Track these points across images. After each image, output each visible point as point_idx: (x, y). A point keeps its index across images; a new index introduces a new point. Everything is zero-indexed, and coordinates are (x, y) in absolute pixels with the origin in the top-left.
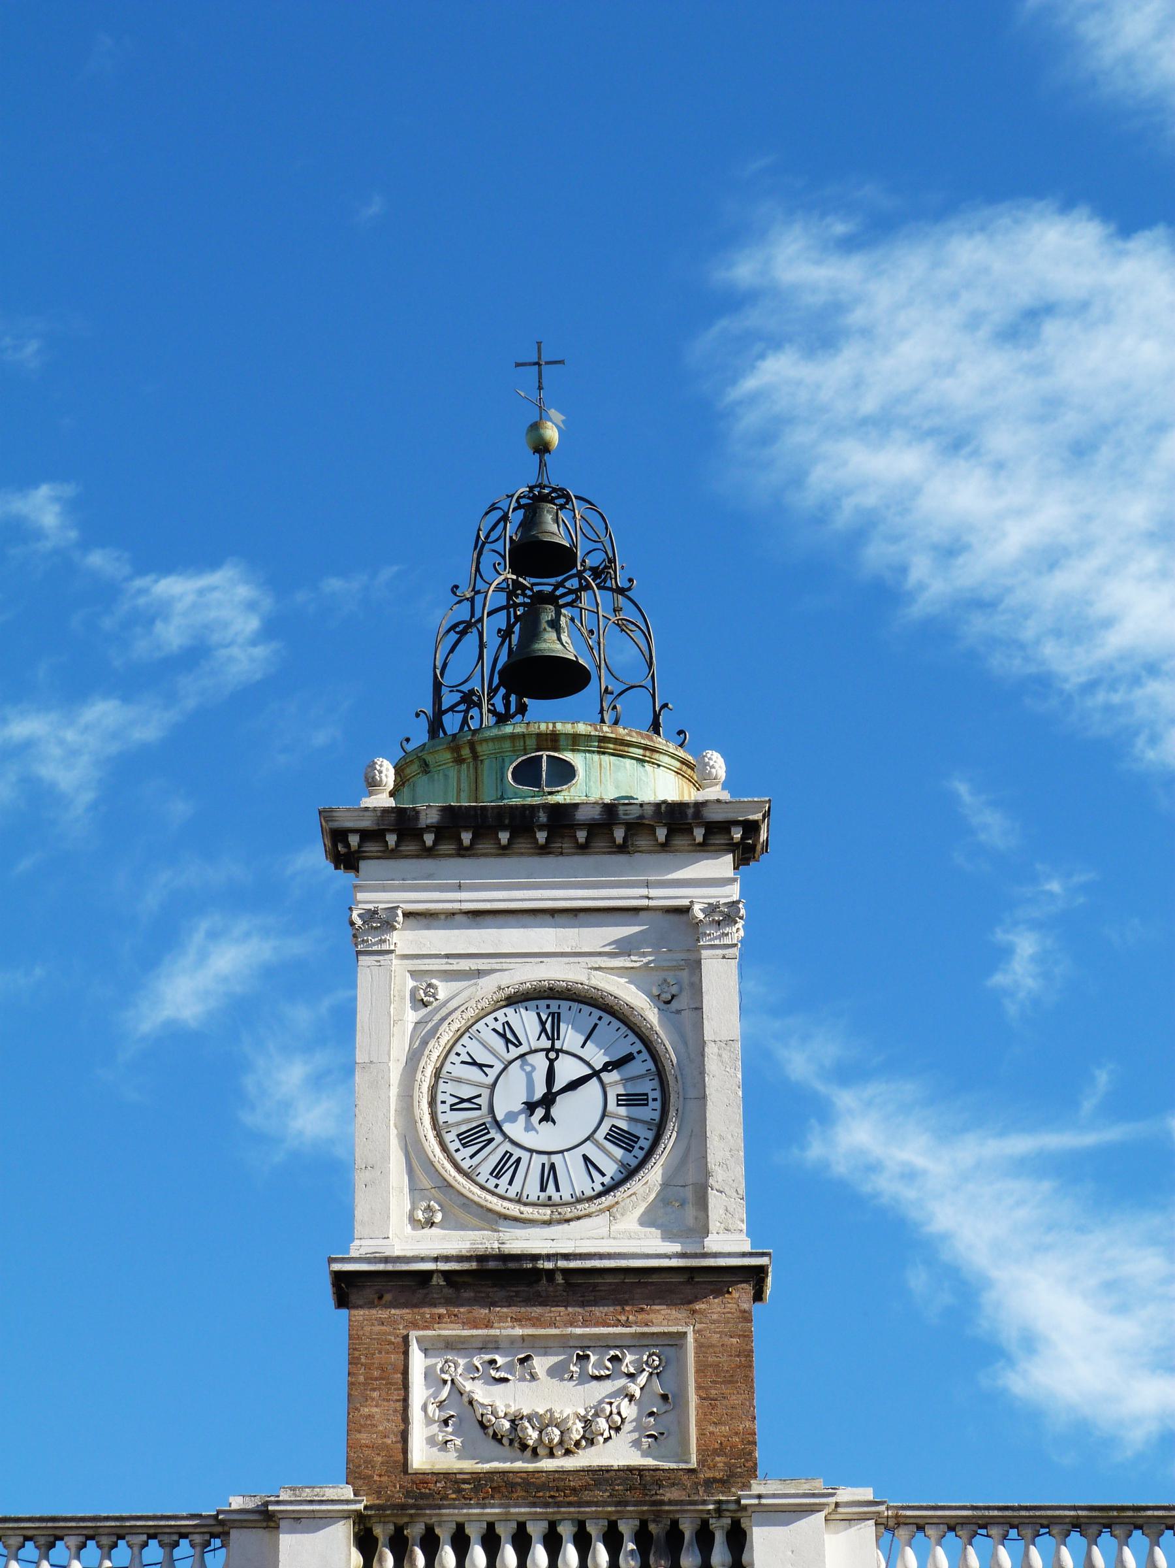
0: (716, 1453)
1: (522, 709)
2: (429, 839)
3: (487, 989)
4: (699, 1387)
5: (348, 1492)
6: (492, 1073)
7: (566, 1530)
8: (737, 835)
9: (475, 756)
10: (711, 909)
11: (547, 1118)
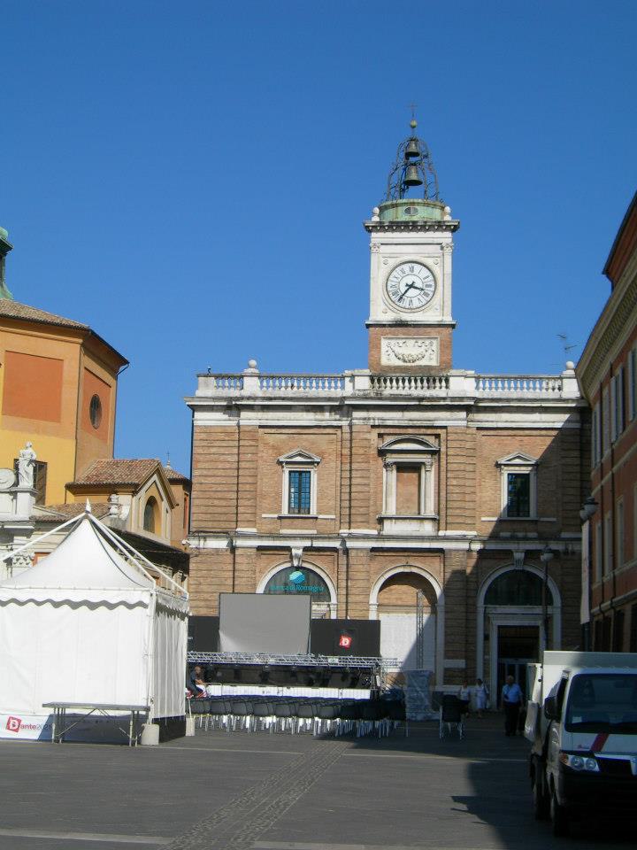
3: (399, 261)
5: (368, 371)
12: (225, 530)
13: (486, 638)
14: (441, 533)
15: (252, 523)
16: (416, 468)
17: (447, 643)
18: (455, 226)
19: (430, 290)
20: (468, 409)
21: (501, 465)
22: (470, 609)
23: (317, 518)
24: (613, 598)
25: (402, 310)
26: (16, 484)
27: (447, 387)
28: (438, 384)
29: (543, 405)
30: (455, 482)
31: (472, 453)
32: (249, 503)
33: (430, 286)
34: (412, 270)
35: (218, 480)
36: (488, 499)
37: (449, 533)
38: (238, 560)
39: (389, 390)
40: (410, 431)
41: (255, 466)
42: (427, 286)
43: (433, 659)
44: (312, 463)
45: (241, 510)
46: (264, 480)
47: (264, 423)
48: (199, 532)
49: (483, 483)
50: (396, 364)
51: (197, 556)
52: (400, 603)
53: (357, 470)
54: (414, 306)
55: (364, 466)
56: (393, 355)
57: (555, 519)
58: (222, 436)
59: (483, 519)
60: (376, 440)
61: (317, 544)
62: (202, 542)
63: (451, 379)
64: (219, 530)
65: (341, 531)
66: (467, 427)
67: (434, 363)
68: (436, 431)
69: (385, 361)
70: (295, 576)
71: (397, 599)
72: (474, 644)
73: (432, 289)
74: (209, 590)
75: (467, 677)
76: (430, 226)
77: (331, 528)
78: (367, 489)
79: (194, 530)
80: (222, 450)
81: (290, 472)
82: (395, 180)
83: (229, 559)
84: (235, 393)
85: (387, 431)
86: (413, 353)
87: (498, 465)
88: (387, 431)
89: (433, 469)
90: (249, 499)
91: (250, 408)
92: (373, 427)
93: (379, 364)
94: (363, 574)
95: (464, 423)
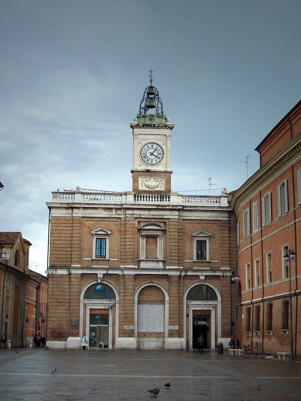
0: (167, 189)
1: (148, 109)
2: (141, 127)
3: (147, 142)
4: (166, 183)
6: (147, 151)
7: (153, 196)
8: (171, 128)
9: (145, 117)
10: (169, 135)
11: (151, 155)
12: (65, 266)
13: (187, 315)
14: (167, 267)
15: (79, 262)
16: (155, 237)
17: (170, 318)
18: (172, 127)
19: (160, 156)
20: (179, 210)
21: (194, 236)
22: (180, 302)
24: (263, 297)
25: (149, 165)
27: (169, 201)
28: (165, 199)
29: (213, 209)
30: (173, 244)
32: (77, 253)
33: (161, 154)
34: (152, 146)
35: (62, 242)
36: (187, 252)
37: (171, 267)
38: (72, 280)
39: (143, 202)
40: (153, 220)
41: (80, 236)
42: (159, 154)
43: (163, 326)
44: (107, 234)
45: (73, 256)
46: (85, 242)
47: (84, 215)
48: (53, 266)
49: (185, 245)
50: (146, 190)
51: (52, 278)
52: (147, 300)
53: (128, 238)
54: (153, 163)
55: (131, 236)
56: (144, 185)
57: (217, 261)
58: (64, 222)
59: (186, 261)
60: (137, 224)
61: (110, 272)
62: (54, 271)
63: (171, 197)
64: (63, 266)
65: (121, 266)
66: (179, 219)
67: (163, 189)
68: (164, 221)
69: (140, 188)
70: (99, 287)
71: (146, 298)
72: (183, 318)
73: (162, 155)
74: (58, 294)
75: (179, 334)
76: (161, 126)
78: (133, 247)
79: (51, 265)
80: (64, 228)
81: (96, 238)
82: (143, 105)
83: (67, 279)
84: (70, 201)
85: (142, 220)
86: (153, 185)
88: (142, 220)
89: (163, 238)
90: (77, 251)
91: (78, 208)
93: (138, 190)
94: (131, 286)
95: (177, 217)
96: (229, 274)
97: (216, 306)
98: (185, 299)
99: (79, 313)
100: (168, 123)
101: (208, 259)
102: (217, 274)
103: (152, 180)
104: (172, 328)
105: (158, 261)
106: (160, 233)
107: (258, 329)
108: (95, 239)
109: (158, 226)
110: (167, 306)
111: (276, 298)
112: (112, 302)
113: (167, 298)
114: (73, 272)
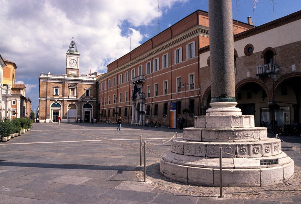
13: (83, 112)
14: (77, 98)
15: (49, 96)
16: (74, 89)
20: (81, 81)
23: (59, 96)
26: (7, 89)
31: (82, 87)
44: (58, 88)
61: (59, 99)
63: (79, 77)
72: (81, 113)
77: (61, 97)
84: (47, 77)
87: (85, 89)
92: (68, 83)
96: (96, 100)
97: (91, 110)
98: (82, 108)
99: (49, 111)
100: (78, 54)
101: (89, 96)
102: (92, 100)
103: (73, 71)
104: (78, 116)
105: (74, 96)
106: (75, 88)
107: (105, 116)
108: (55, 89)
109: (75, 85)
110: (77, 110)
111: (111, 108)
112: (60, 108)
113: (77, 107)
114: (48, 99)
